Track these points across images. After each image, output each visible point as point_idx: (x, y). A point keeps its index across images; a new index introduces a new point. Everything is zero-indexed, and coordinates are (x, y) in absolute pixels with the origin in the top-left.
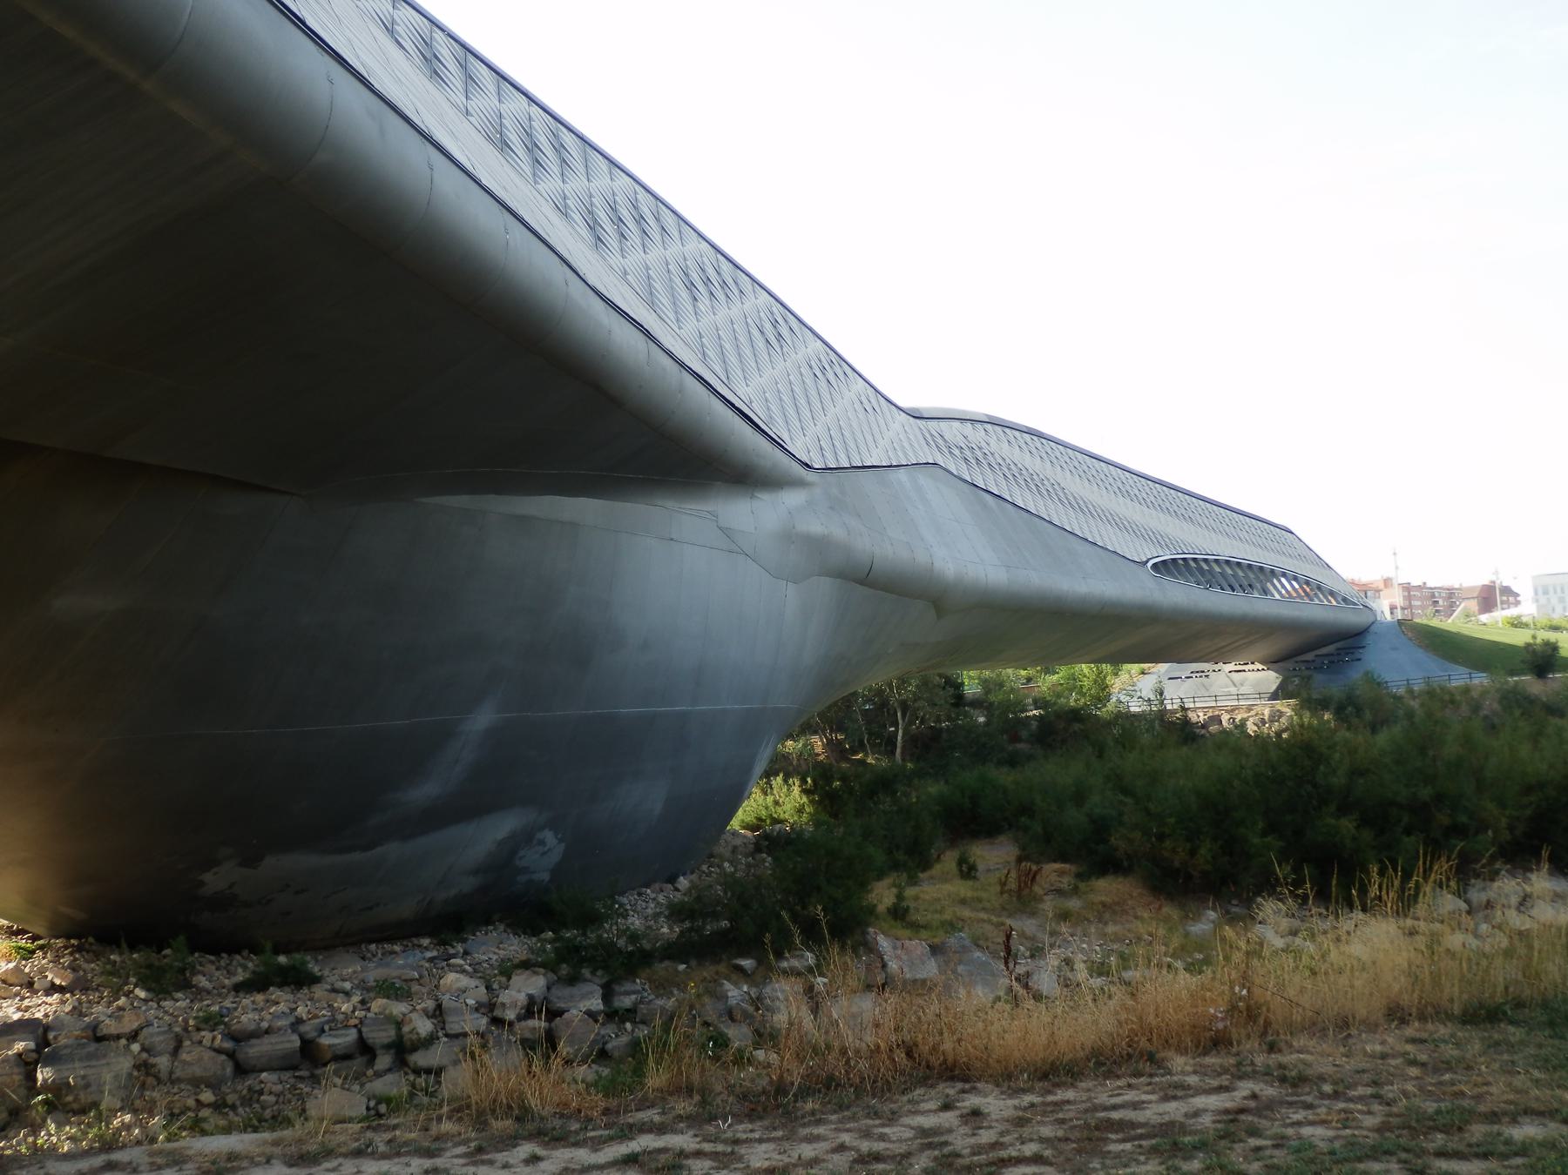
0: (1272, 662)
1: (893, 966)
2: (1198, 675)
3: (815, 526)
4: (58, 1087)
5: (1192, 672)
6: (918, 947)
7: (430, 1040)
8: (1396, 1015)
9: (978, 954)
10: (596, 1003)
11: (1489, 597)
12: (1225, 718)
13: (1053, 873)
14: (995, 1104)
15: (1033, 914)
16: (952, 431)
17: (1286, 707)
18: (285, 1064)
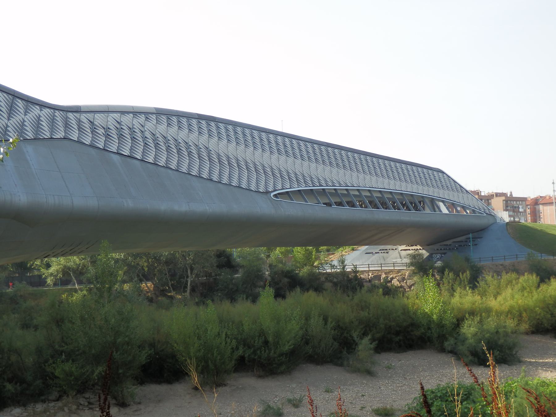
2: (382, 251)
5: (380, 250)
11: (493, 209)
12: (383, 276)
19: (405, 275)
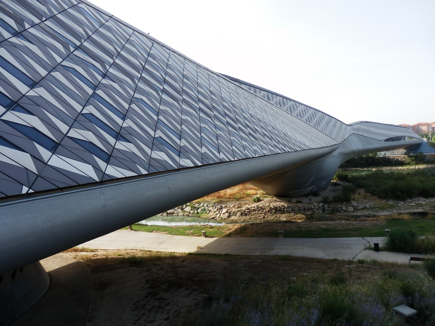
0: (405, 149)
1: (353, 204)
3: (341, 151)
4: (287, 211)
6: (355, 202)
7: (314, 209)
8: (383, 219)
9: (361, 203)
10: (327, 206)
14: (369, 222)
15: (366, 199)
16: (355, 126)
17: (406, 156)
18: (303, 210)
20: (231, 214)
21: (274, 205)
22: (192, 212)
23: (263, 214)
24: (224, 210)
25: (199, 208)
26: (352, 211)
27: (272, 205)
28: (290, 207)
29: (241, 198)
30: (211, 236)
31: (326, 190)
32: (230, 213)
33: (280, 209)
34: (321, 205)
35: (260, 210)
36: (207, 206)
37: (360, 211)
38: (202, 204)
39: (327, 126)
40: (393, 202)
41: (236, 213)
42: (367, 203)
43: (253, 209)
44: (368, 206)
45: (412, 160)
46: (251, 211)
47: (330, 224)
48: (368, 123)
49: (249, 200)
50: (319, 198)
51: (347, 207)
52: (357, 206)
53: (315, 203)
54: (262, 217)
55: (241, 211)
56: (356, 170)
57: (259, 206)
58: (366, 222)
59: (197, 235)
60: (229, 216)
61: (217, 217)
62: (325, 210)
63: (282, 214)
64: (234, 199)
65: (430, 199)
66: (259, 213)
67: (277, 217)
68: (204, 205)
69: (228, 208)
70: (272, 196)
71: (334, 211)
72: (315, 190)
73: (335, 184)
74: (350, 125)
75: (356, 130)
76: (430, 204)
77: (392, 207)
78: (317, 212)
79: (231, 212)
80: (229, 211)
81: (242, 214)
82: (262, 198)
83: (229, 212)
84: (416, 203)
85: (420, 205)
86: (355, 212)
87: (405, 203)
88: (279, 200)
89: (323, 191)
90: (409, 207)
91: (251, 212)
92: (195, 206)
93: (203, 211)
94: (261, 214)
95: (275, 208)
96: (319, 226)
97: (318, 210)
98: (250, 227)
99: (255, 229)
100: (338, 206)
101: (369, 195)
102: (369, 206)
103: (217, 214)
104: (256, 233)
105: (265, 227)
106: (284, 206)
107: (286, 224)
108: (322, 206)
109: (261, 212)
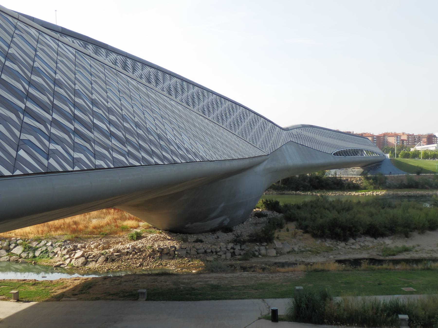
0: (362, 167)
1: (277, 245)
4: (178, 254)
6: (280, 243)
8: (301, 271)
9: (288, 244)
10: (239, 248)
12: (349, 179)
13: (300, 232)
14: (281, 274)
16: (294, 132)
17: (362, 177)
19: (357, 179)
20: (89, 260)
21: (159, 246)
22: (24, 255)
23: (141, 260)
24: (79, 253)
25: (38, 248)
26: (273, 256)
27: (157, 246)
28: (183, 249)
29: (110, 234)
30: (27, 300)
31: (245, 223)
32: (88, 258)
33: (168, 252)
34: (231, 245)
35: (136, 253)
36: (52, 245)
37: (285, 256)
38: (43, 242)
39: (250, 128)
40: (331, 243)
41: (97, 257)
42: (295, 245)
43: (126, 251)
44: (296, 249)
45: (369, 183)
46: (123, 254)
47: (225, 278)
48: (313, 128)
49: (123, 237)
50: (230, 236)
51: (268, 249)
52: (281, 248)
53: (222, 244)
54: (138, 265)
55: (106, 254)
56: (296, 194)
57: (137, 247)
58: (278, 274)
59: (4, 297)
60: (86, 263)
61: (65, 264)
62: (236, 254)
63: (170, 259)
64: (99, 235)
65: (379, 239)
66: (135, 258)
67: (161, 265)
68: (46, 244)
69: (87, 250)
70: (161, 231)
71: (247, 257)
72: (226, 223)
73: (259, 215)
74: (287, 129)
75: (295, 136)
76: (379, 247)
77: (329, 250)
78: (223, 256)
79: (89, 255)
80: (86, 255)
81: (107, 260)
82: (144, 234)
83: (86, 256)
84: (361, 246)
85: (364, 248)
86: (278, 257)
87: (347, 245)
88: (169, 238)
89: (239, 224)
90: (351, 250)
91: (122, 255)
92: (30, 245)
93: (44, 253)
94: (138, 259)
95: (160, 250)
96: (208, 281)
97: (225, 253)
98: (100, 283)
99: (107, 286)
100: (255, 248)
101: (301, 232)
102: (298, 249)
103: (65, 259)
104: (105, 293)
105: (125, 283)
106: (175, 248)
107: (160, 277)
108: (232, 248)
109: (138, 256)
